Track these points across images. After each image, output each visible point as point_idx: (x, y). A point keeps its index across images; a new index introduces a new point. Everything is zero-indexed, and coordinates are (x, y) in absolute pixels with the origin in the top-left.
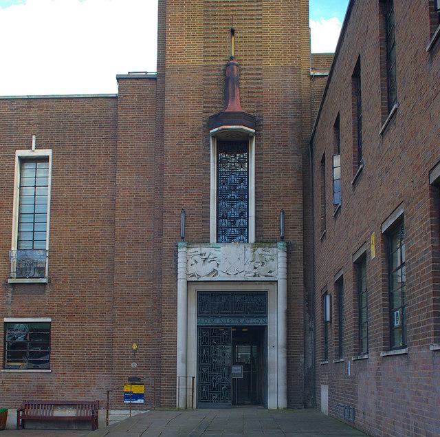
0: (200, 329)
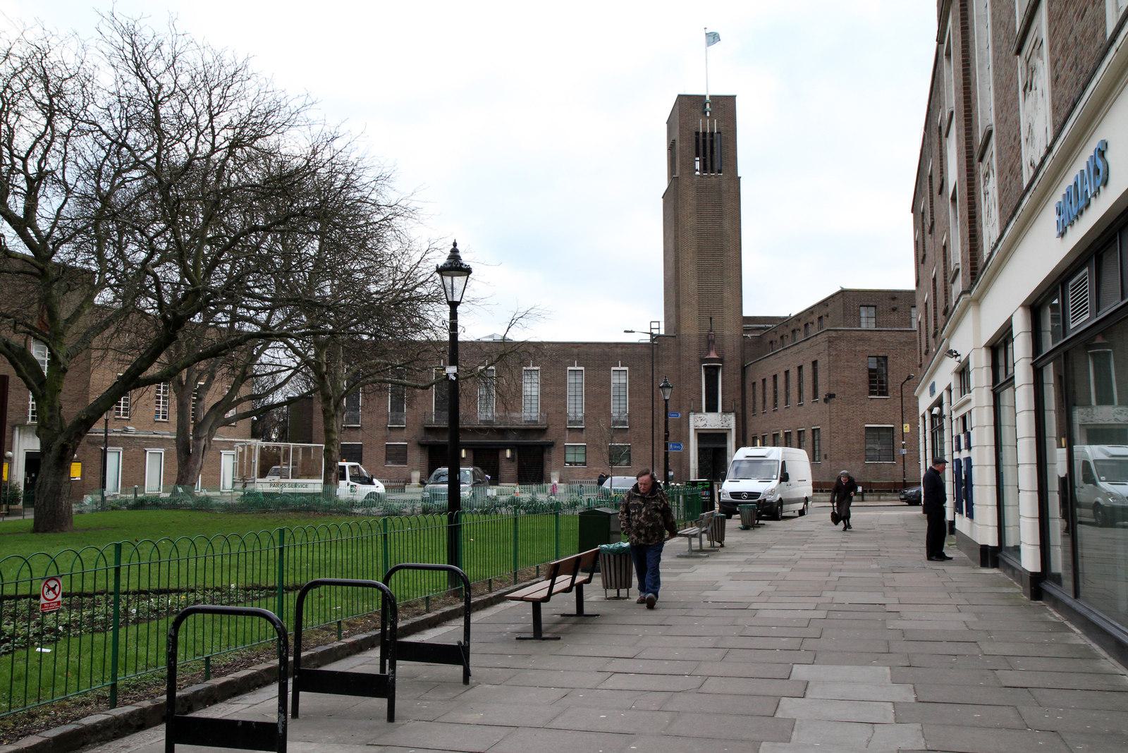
0: (699, 449)
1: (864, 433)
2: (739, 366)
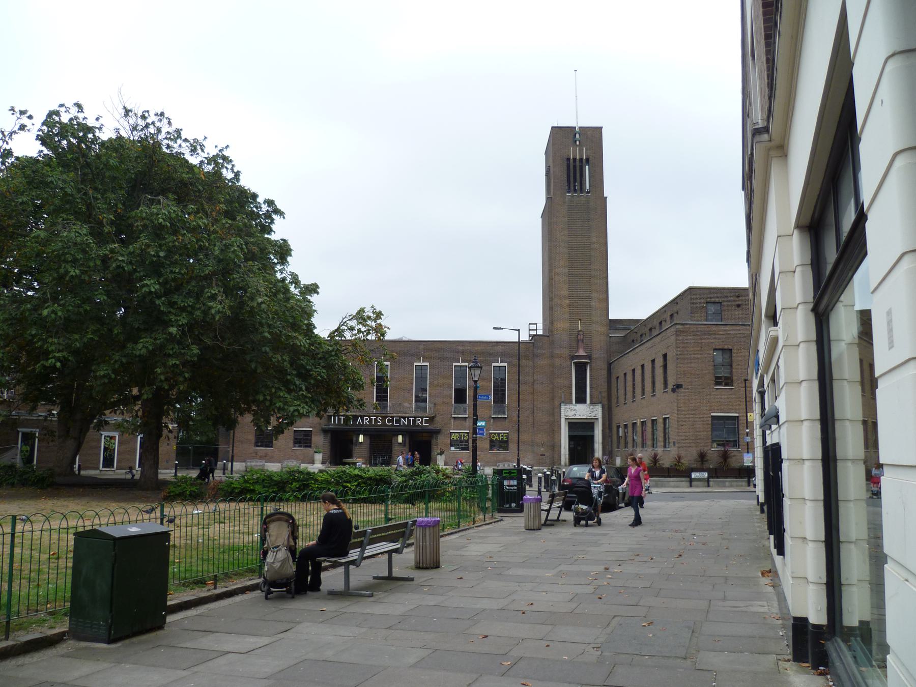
1: (710, 421)
2: (606, 363)
